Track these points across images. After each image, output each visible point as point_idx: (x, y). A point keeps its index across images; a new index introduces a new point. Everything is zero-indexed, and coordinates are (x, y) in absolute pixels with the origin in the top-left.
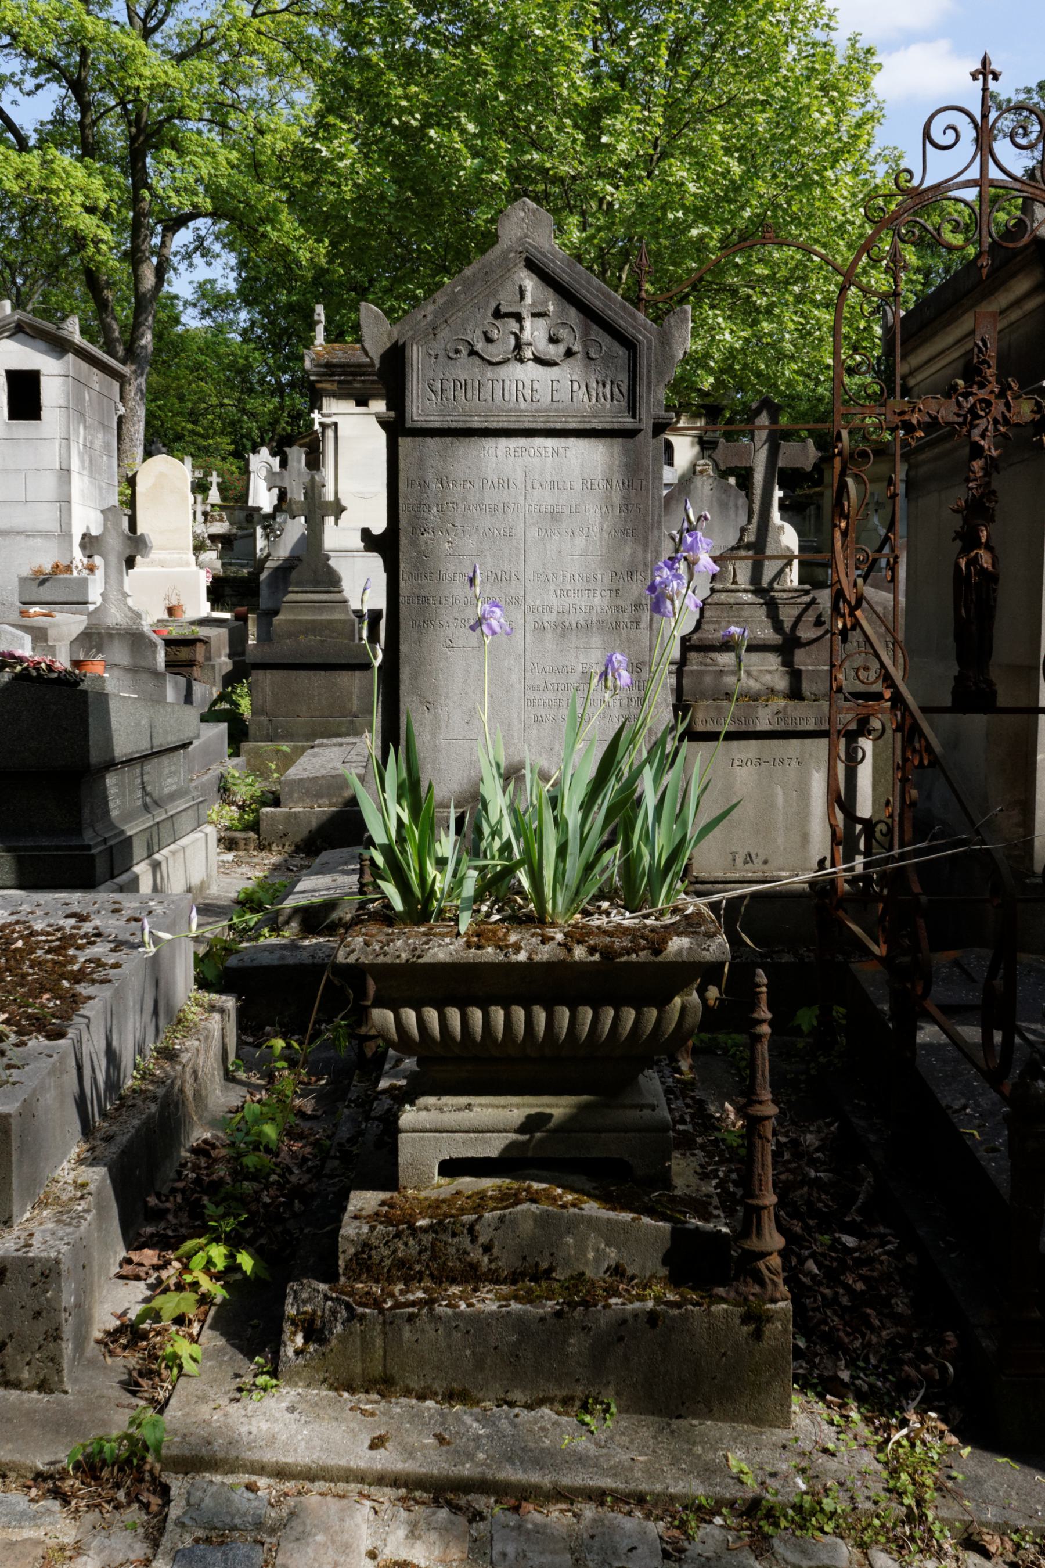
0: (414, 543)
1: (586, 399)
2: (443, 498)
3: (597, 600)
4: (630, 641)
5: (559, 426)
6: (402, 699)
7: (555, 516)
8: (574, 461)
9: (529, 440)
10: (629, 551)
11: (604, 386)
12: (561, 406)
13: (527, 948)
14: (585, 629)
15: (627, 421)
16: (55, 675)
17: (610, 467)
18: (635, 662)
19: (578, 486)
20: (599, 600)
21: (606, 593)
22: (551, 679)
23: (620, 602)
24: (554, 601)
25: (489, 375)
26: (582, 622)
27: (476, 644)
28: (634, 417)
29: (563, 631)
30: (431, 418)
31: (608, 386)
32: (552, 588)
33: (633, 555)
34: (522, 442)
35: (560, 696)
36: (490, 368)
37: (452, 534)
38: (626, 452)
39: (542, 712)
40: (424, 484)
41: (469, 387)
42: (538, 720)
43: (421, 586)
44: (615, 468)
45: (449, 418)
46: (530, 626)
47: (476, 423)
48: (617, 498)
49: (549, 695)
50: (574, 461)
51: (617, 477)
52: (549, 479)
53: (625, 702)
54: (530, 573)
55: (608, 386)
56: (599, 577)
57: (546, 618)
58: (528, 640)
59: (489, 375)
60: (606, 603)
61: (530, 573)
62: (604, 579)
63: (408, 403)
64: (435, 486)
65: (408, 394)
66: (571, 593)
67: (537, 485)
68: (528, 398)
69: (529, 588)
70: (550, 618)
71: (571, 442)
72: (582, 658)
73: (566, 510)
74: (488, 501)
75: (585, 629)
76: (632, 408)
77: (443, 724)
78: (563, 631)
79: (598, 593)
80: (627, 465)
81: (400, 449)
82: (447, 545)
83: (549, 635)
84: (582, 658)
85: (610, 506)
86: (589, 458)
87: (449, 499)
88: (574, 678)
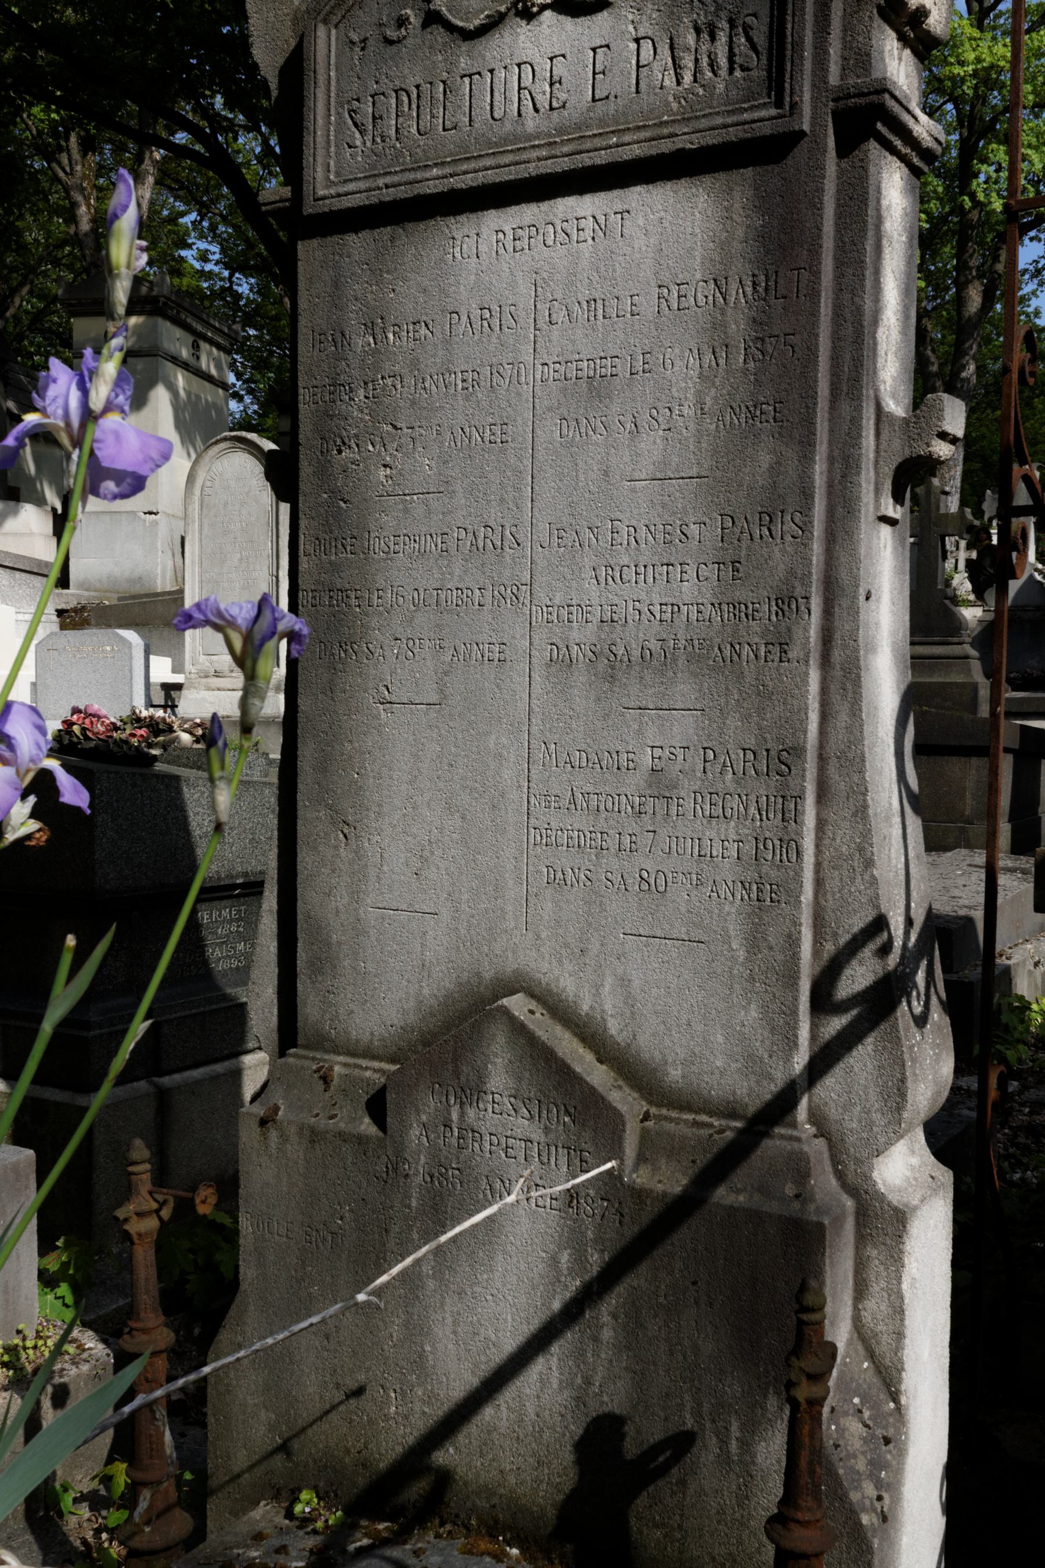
0: (323, 470)
1: (670, 81)
2: (376, 367)
3: (688, 590)
4: (764, 694)
5: (602, 158)
6: (300, 813)
7: (596, 386)
8: (640, 242)
9: (545, 206)
10: (765, 459)
11: (713, 38)
12: (611, 107)
13: (146, 1558)
14: (659, 662)
15: (763, 119)
16: (92, 744)
17: (723, 246)
18: (775, 747)
19: (648, 305)
20: (692, 588)
21: (710, 572)
22: (583, 782)
23: (741, 594)
24: (593, 593)
25: (464, 63)
26: (654, 645)
27: (434, 698)
28: (779, 104)
29: (610, 665)
30: (351, 187)
31: (722, 38)
32: (588, 560)
33: (775, 469)
34: (529, 213)
35: (602, 825)
36: (465, 46)
37: (392, 446)
38: (762, 202)
39: (565, 860)
40: (341, 337)
41: (425, 101)
42: (557, 881)
43: (335, 568)
44: (737, 246)
45: (381, 182)
46: (540, 657)
47: (434, 182)
48: (738, 327)
49: (580, 821)
50: (640, 242)
51: (740, 268)
52: (584, 294)
53: (749, 848)
54: (543, 527)
55: (722, 38)
56: (694, 530)
57: (575, 635)
58: (537, 688)
59: (464, 63)
60: (707, 598)
61: (543, 527)
62: (702, 533)
63: (308, 160)
64: (362, 341)
65: (308, 139)
66: (630, 574)
67: (560, 316)
68: (543, 101)
69: (541, 563)
70: (583, 634)
71: (636, 196)
72: (652, 735)
73: (623, 370)
74: (460, 365)
75: (659, 662)
76: (777, 84)
77: (372, 872)
78: (610, 665)
79: (692, 573)
80: (763, 237)
81: (301, 266)
82: (382, 472)
83: (580, 677)
84: (652, 735)
85: (719, 344)
86: (671, 230)
87: (387, 365)
88: (634, 783)
